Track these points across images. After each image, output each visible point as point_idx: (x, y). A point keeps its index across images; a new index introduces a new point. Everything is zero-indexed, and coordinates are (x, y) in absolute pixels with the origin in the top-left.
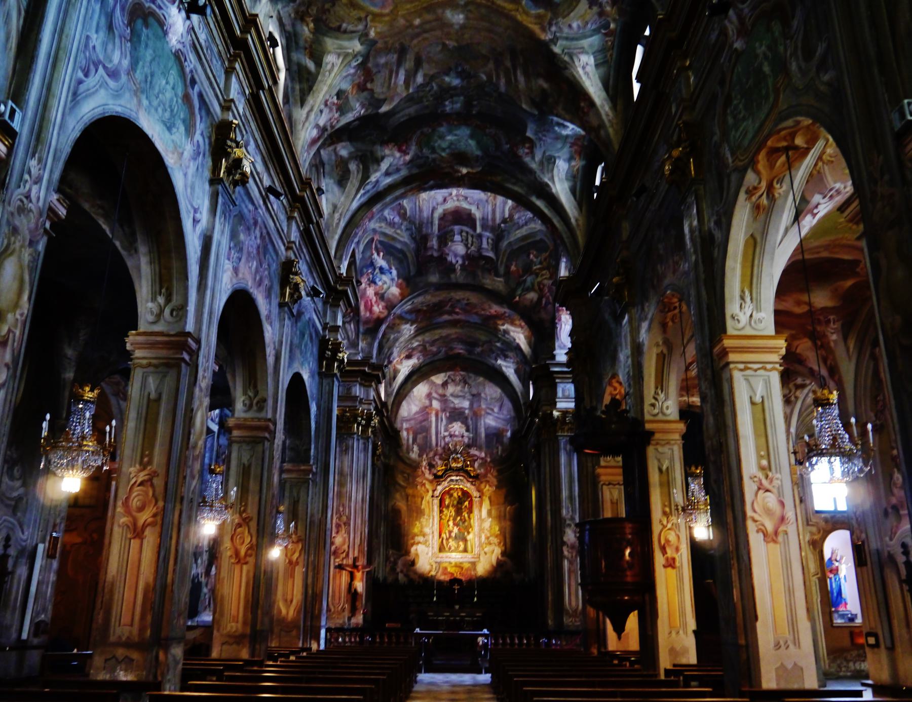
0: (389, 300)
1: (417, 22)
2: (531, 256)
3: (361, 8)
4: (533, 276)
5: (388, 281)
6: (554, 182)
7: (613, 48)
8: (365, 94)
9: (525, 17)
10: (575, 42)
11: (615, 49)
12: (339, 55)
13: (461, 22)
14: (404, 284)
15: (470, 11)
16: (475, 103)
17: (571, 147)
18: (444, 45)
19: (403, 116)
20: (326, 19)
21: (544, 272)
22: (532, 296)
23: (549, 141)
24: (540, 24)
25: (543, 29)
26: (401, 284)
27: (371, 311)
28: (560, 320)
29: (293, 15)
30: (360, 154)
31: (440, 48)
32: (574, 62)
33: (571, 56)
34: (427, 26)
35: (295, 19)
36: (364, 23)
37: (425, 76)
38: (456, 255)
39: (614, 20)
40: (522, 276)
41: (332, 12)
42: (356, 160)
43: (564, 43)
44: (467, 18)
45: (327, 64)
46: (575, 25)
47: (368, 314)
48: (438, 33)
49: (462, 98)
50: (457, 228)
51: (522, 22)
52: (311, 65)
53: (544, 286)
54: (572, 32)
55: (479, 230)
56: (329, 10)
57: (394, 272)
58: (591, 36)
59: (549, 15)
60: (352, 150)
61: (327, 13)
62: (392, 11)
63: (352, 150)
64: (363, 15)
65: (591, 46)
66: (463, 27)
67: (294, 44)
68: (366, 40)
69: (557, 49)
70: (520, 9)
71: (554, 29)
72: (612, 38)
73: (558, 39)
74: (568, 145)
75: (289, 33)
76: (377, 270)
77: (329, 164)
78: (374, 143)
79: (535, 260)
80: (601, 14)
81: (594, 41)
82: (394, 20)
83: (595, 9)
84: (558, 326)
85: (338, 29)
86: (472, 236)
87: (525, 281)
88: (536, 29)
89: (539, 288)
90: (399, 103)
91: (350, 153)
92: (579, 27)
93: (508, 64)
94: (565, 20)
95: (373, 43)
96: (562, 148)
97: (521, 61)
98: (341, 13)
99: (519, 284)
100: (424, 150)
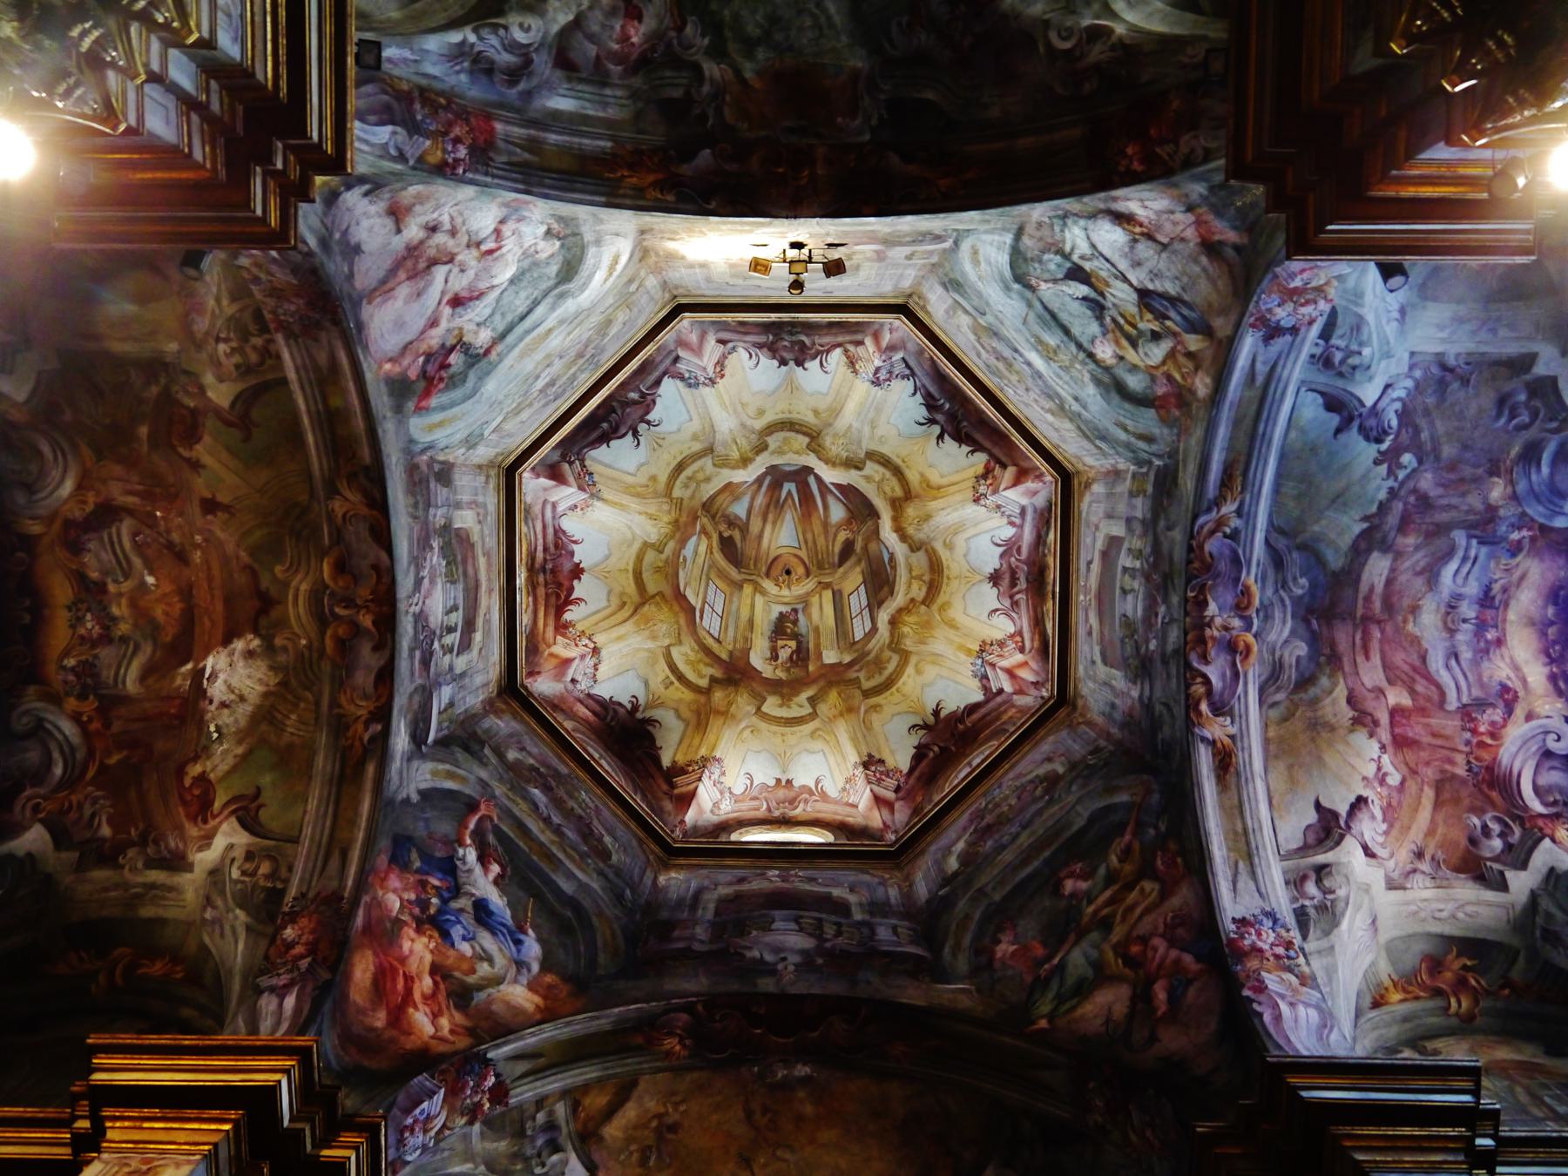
0: (486, 1014)
2: (1069, 885)
4: (1094, 936)
5: (500, 961)
6: (1114, 15)
14: (564, 990)
21: (1133, 896)
22: (1110, 1001)
26: (550, 987)
27: (398, 1016)
28: (1261, 988)
38: (777, 950)
40: (1049, 958)
47: (380, 1019)
50: (777, 913)
53: (1144, 940)
55: (858, 916)
57: (532, 948)
76: (463, 903)
79: (1083, 885)
84: (1255, 1006)
86: (839, 925)
87: (1061, 967)
89: (1130, 961)
99: (1041, 984)
100: (689, 30)
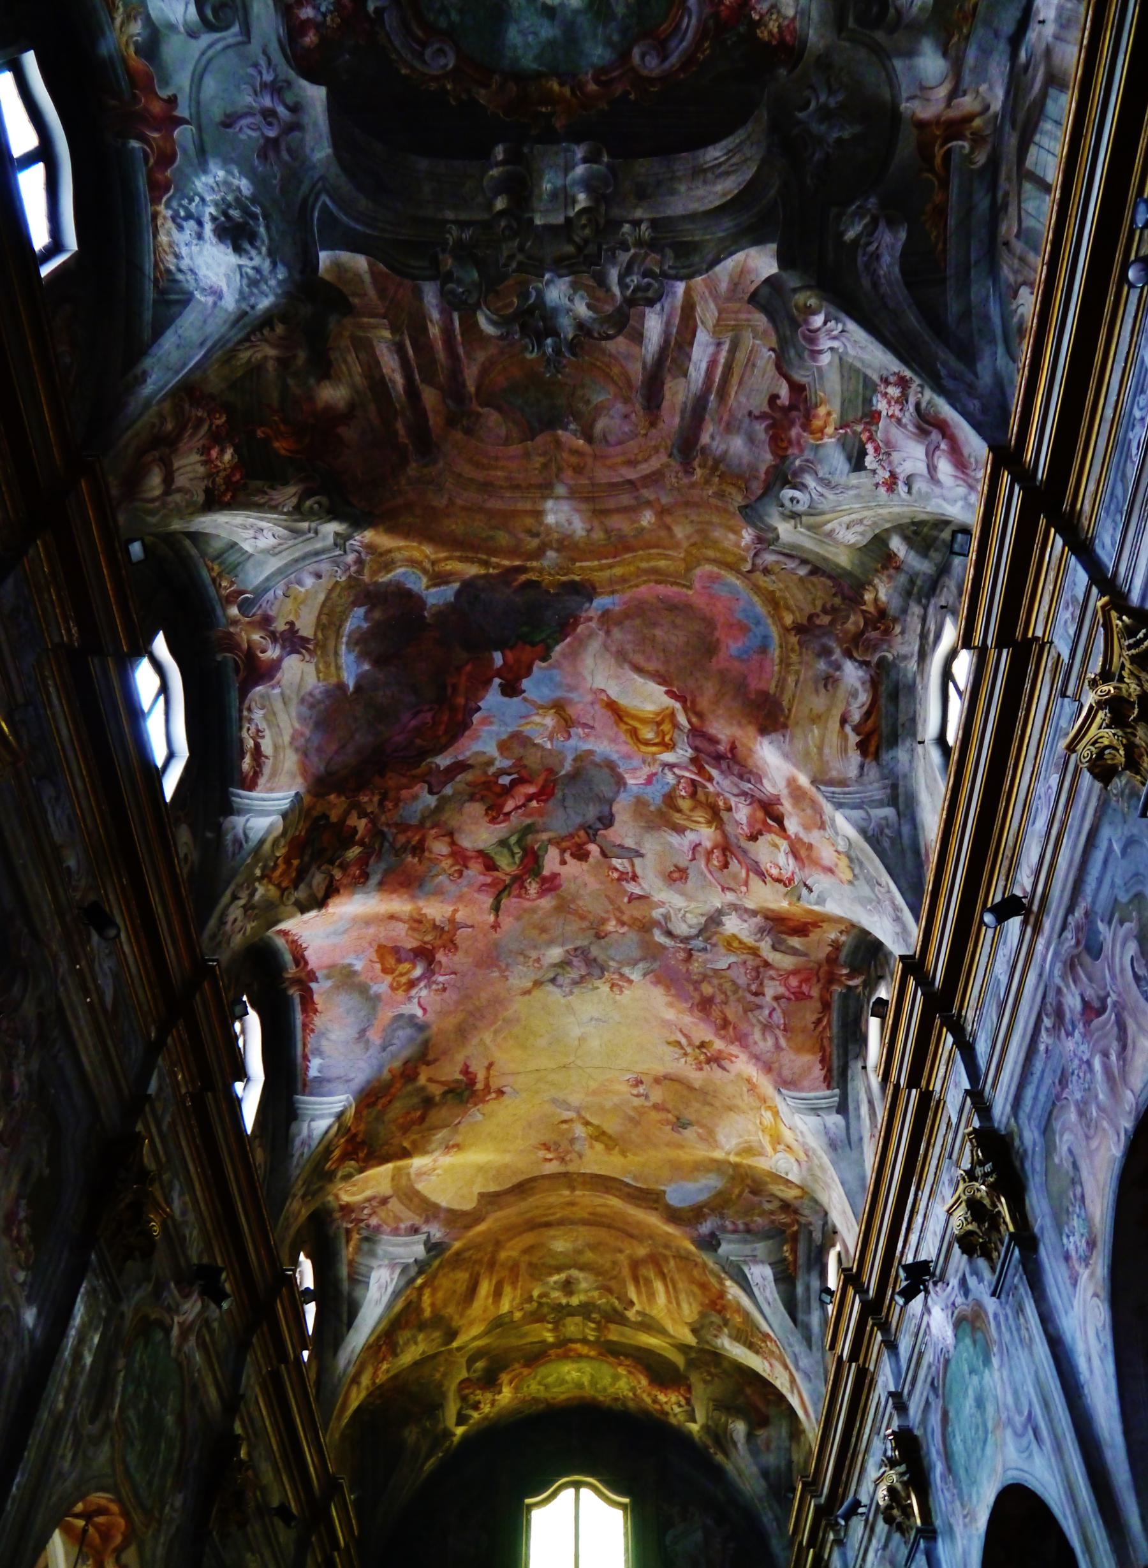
1: (647, 518)
3: (756, 589)
7: (214, 580)
8: (799, 376)
9: (417, 555)
10: (297, 555)
11: (208, 581)
12: (830, 534)
13: (549, 504)
15: (536, 535)
16: (500, 204)
17: (172, 101)
18: (589, 439)
19: (717, 172)
20: (835, 595)
23: (249, 99)
24: (381, 555)
25: (370, 548)
29: (898, 629)
30: (880, 36)
31: (600, 425)
32: (286, 528)
33: (292, 531)
34: (626, 499)
35: (895, 620)
36: (759, 561)
37: (638, 337)
39: (235, 622)
41: (819, 603)
42: (899, 12)
43: (319, 545)
44: (539, 514)
45: (862, 534)
46: (309, 581)
48: (603, 476)
49: (538, 221)
51: (420, 543)
52: (897, 544)
54: (311, 568)
56: (825, 611)
58: (268, 579)
59: (366, 578)
60: (899, 64)
61: (828, 606)
62: (699, 565)
63: (899, 64)
64: (758, 576)
65: (261, 564)
66: (545, 489)
67: (919, 582)
68: (761, 529)
69: (332, 528)
70: (428, 566)
71: (351, 558)
72: (224, 593)
73: (336, 545)
74: (183, 111)
75: (919, 602)
77: (997, 35)
78: (824, 63)
80: (265, 622)
81: (254, 577)
82: (694, 544)
83: (280, 626)
85: (815, 571)
88: (385, 541)
90: (717, 261)
91: (911, 53)
92: (300, 583)
93: (429, 396)
94: (334, 580)
95: (750, 513)
96: (198, 80)
97: (399, 426)
98: (800, 596)
